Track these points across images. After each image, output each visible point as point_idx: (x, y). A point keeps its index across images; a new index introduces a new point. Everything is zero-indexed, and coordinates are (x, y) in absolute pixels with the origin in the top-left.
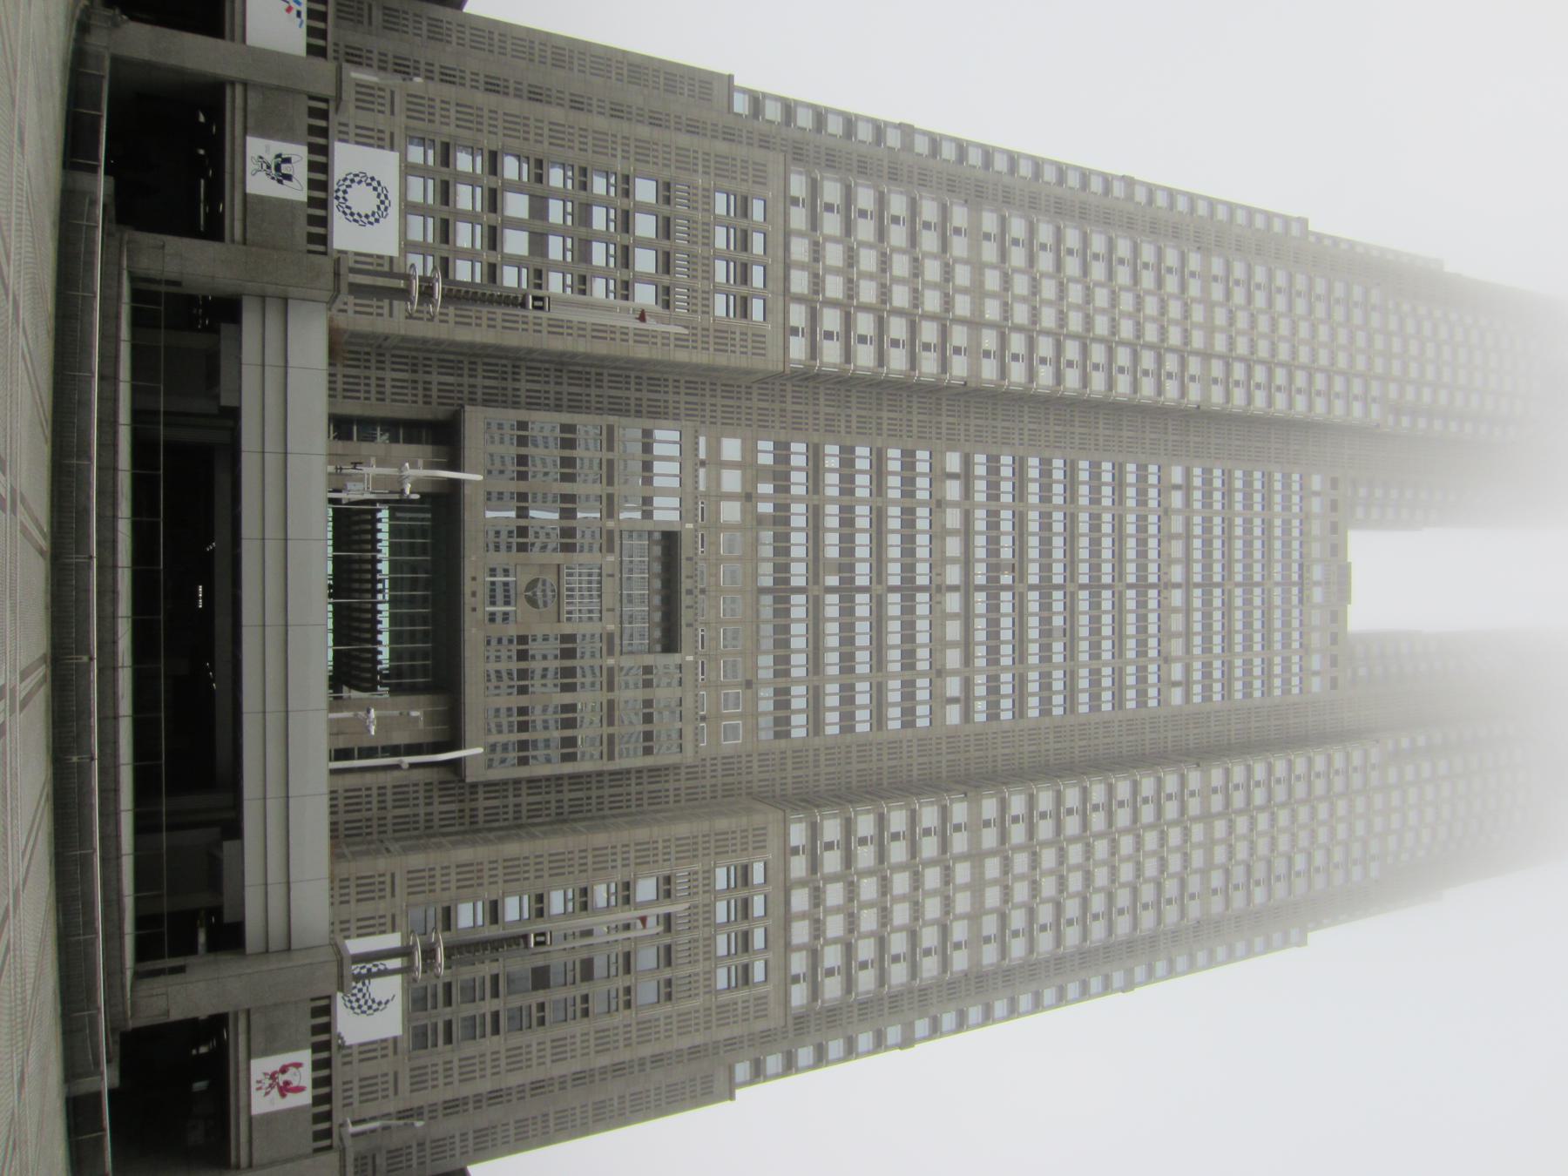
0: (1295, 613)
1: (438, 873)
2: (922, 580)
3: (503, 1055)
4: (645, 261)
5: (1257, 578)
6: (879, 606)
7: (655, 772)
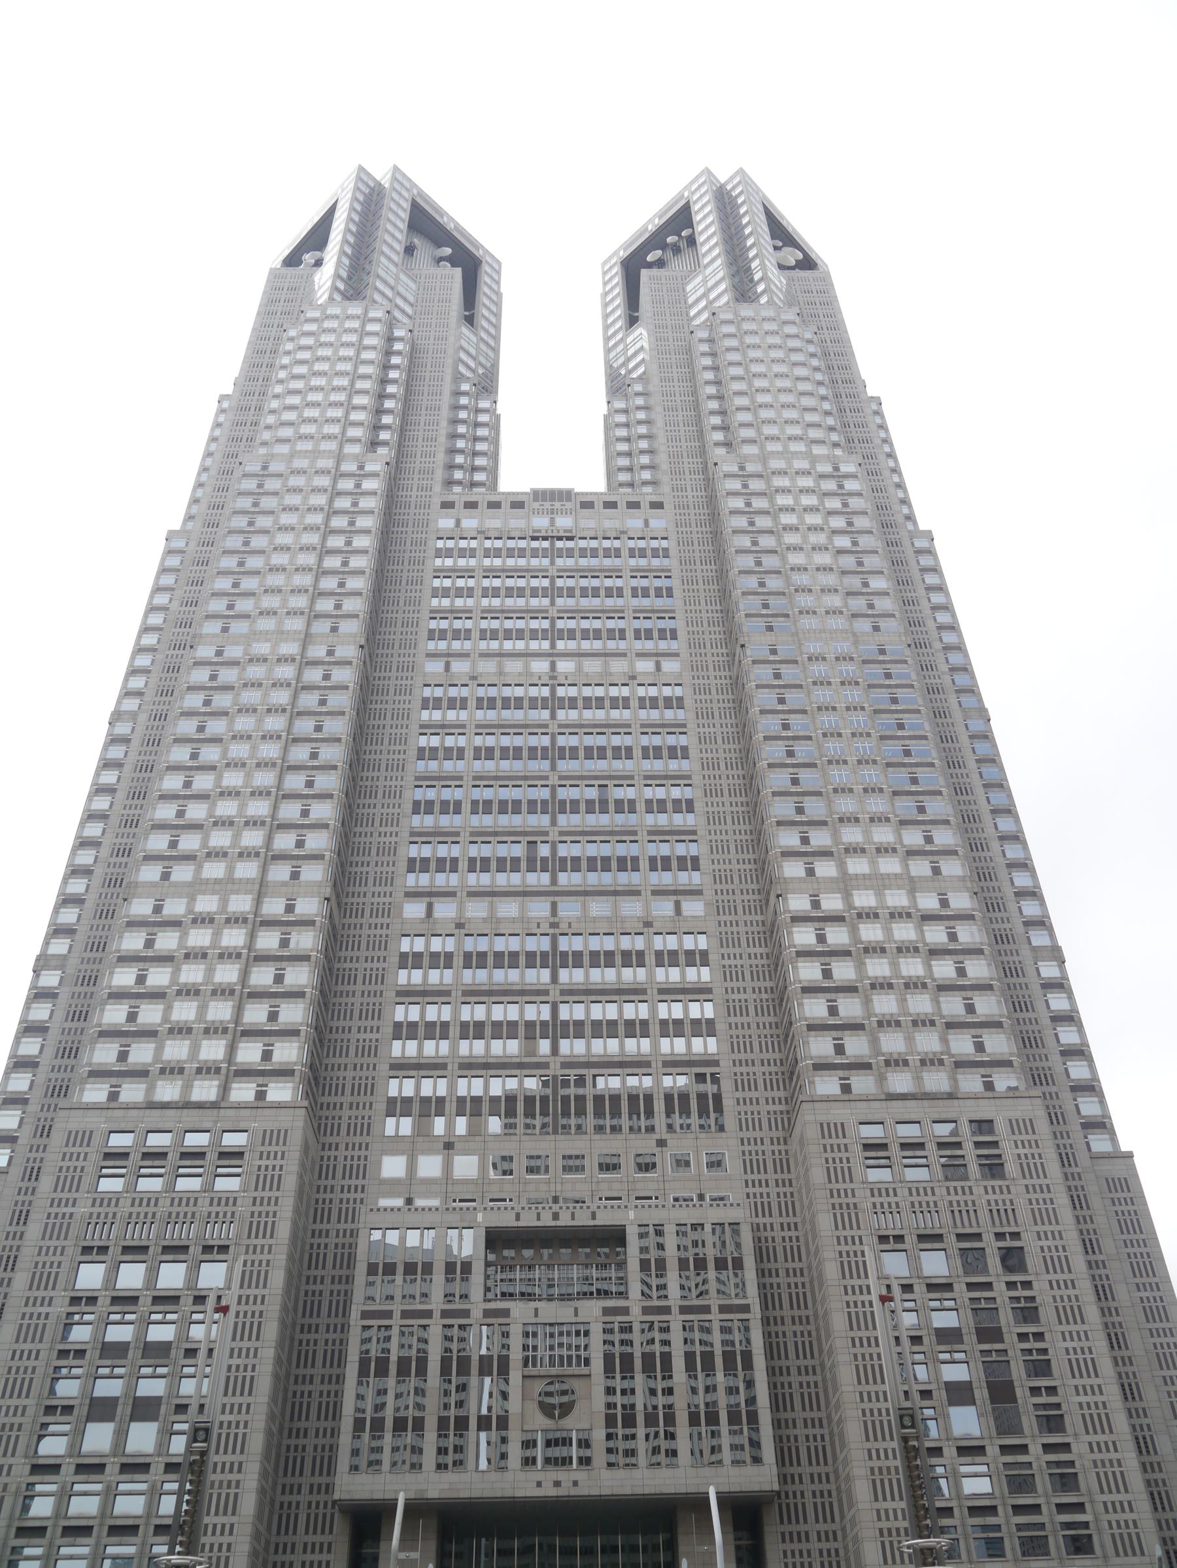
0: (583, 544)
1: (884, 1525)
2: (545, 944)
3: (1094, 1438)
4: (172, 1276)
5: (546, 583)
6: (574, 993)
7: (761, 1254)
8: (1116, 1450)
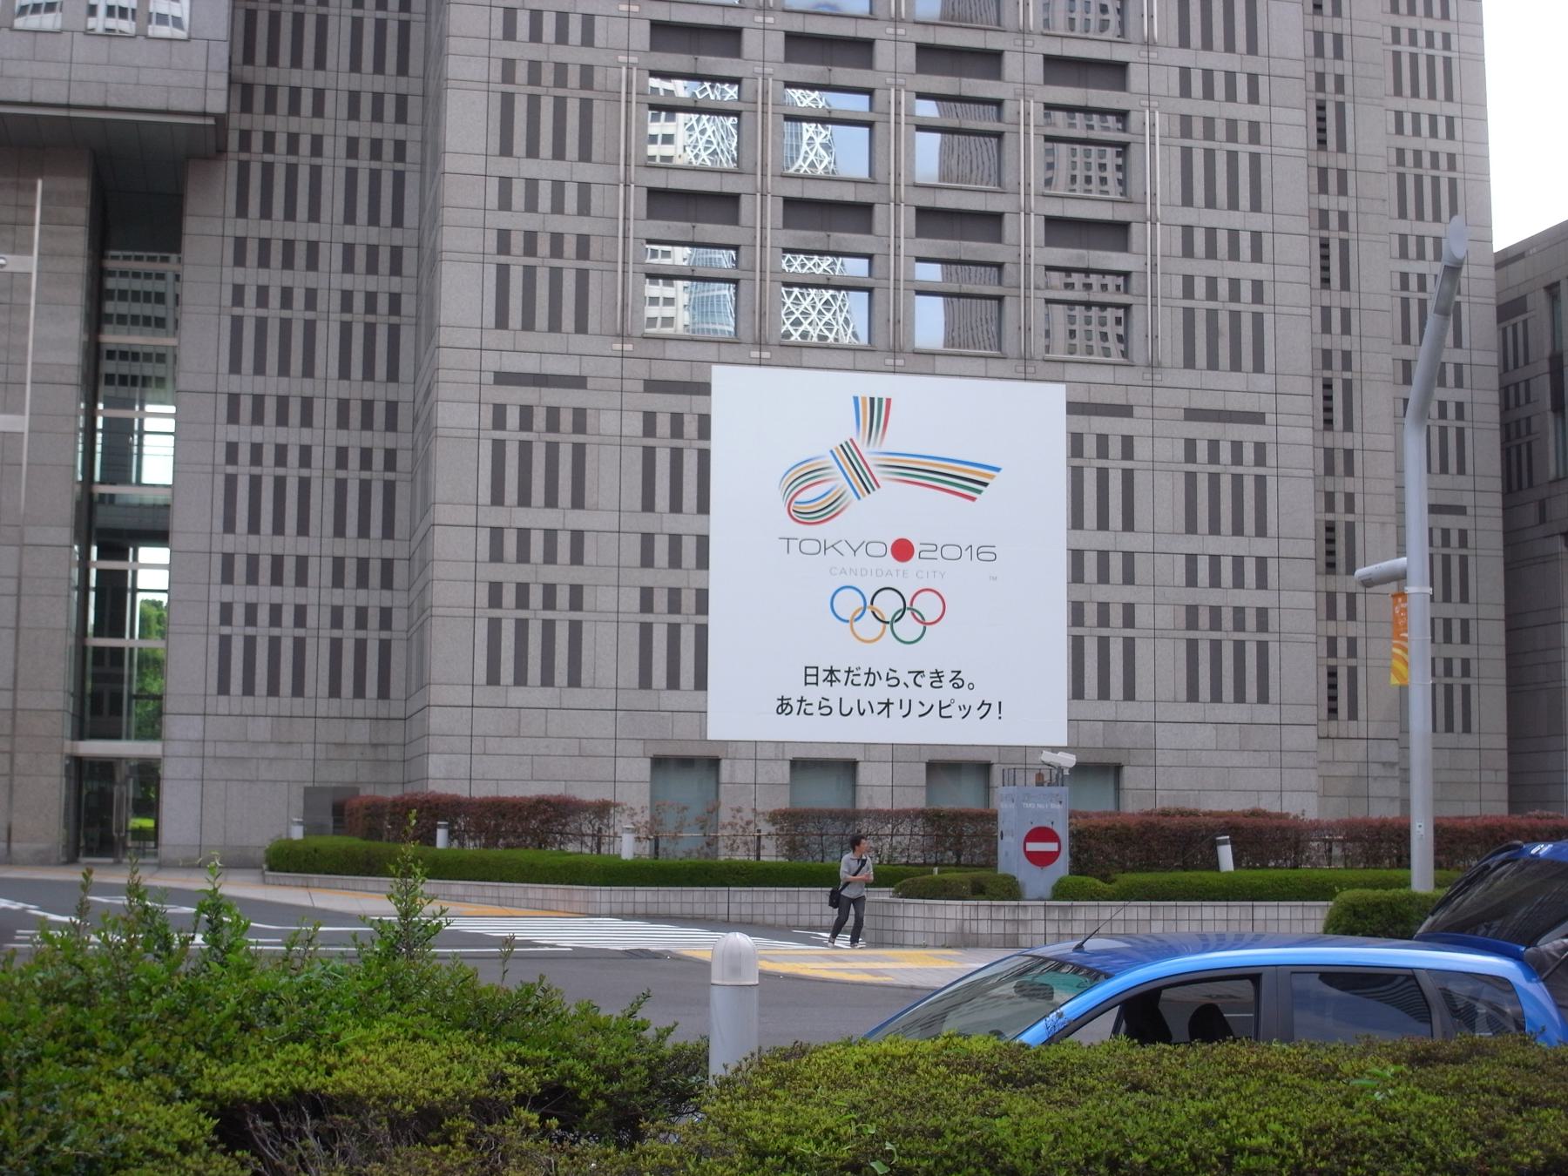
3: (1196, 59)
8: (1253, 98)
